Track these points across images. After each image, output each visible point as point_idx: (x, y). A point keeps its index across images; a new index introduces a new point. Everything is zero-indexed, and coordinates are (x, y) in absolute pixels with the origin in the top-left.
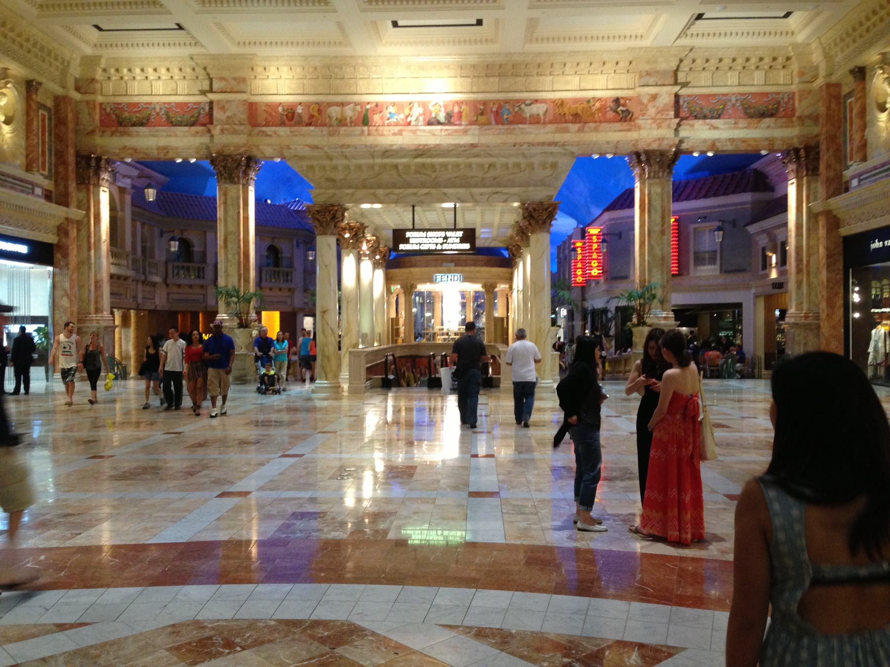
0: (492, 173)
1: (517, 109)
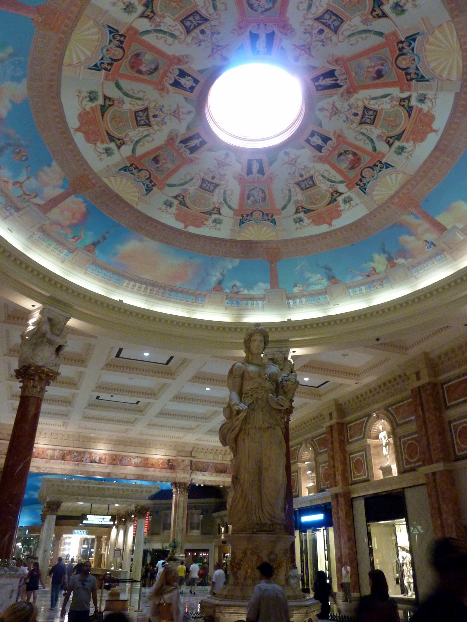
0: (126, 493)
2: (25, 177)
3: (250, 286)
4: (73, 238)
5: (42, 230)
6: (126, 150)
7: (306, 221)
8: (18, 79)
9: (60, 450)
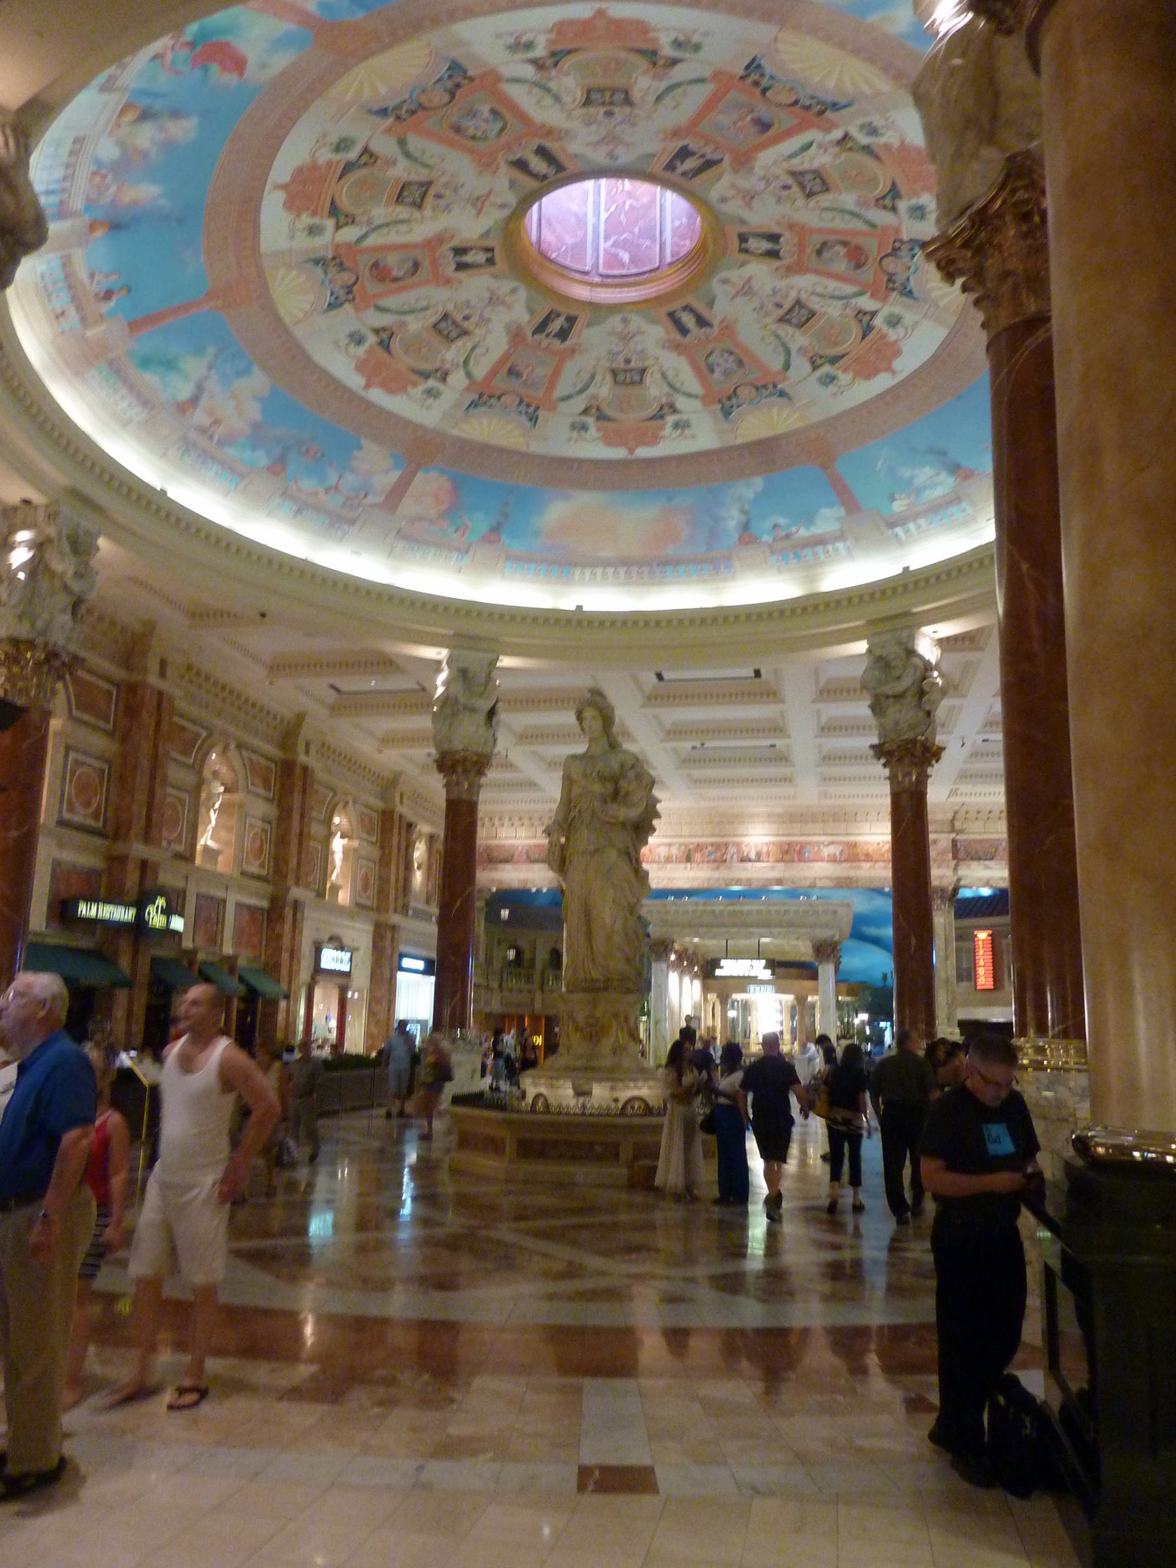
1: (816, 849)
3: (808, 518)
5: (400, 535)
6: (458, 379)
7: (844, 378)
8: (247, 371)
9: (681, 845)
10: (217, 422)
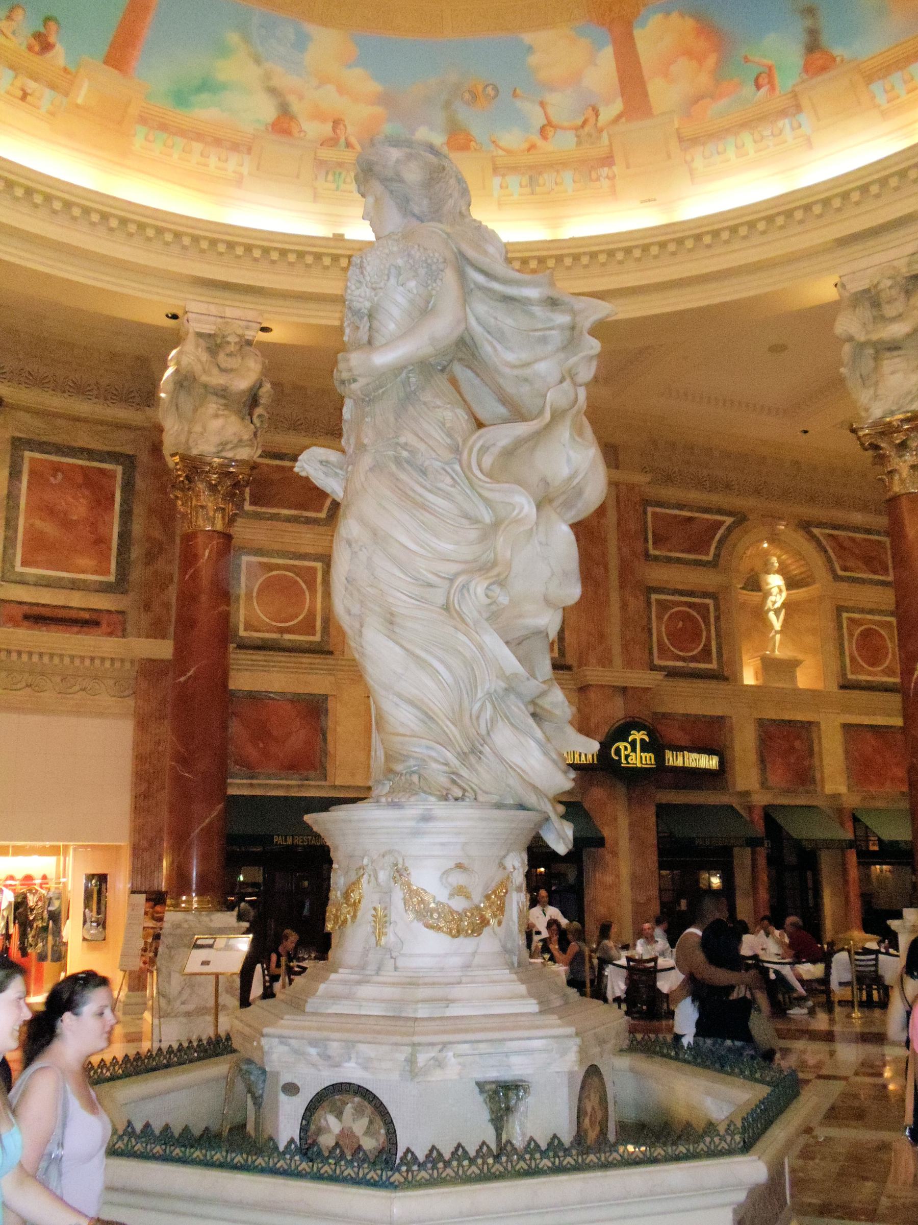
2: (538, 110)
4: (758, 87)
10: (337, 123)
